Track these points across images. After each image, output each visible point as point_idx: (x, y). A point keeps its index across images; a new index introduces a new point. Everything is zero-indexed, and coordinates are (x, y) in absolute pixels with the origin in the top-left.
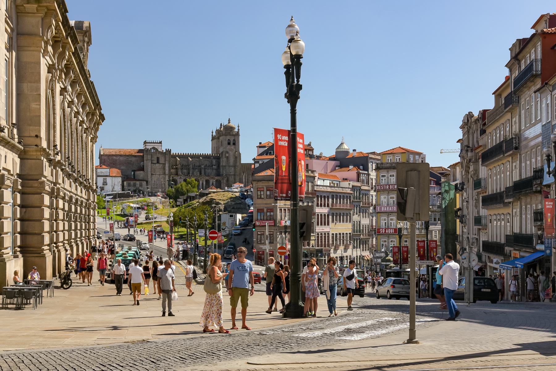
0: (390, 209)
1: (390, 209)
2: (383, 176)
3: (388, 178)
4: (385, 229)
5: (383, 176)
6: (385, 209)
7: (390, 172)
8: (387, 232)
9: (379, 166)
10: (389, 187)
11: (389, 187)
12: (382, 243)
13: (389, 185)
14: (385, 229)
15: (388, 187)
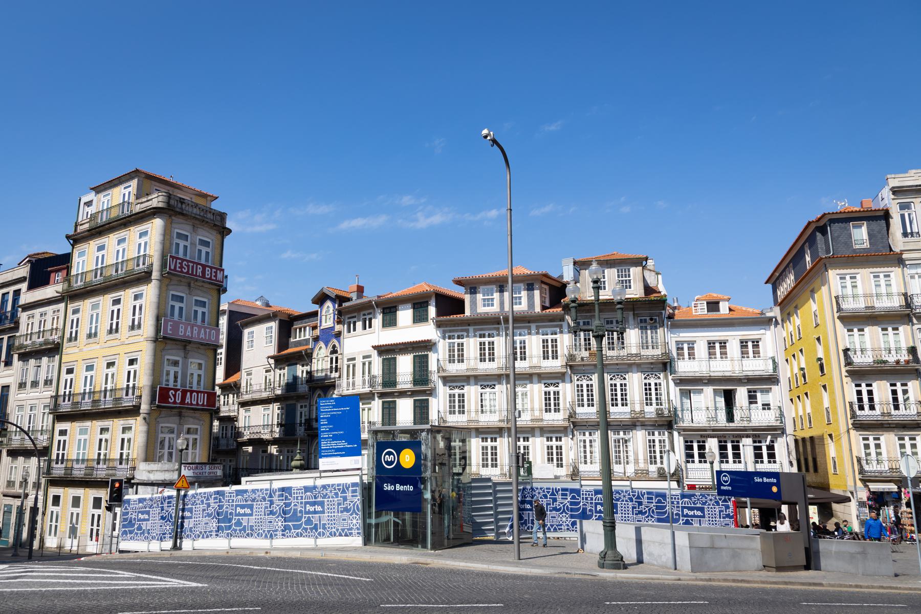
0: (202, 336)
1: (202, 336)
2: (180, 236)
3: (193, 244)
4: (184, 393)
5: (180, 236)
6: (188, 333)
7: (200, 231)
8: (188, 400)
9: (172, 202)
10: (204, 272)
11: (204, 272)
12: (161, 436)
13: (204, 267)
14: (184, 393)
15: (200, 271)
